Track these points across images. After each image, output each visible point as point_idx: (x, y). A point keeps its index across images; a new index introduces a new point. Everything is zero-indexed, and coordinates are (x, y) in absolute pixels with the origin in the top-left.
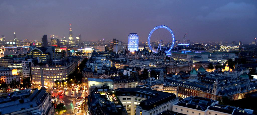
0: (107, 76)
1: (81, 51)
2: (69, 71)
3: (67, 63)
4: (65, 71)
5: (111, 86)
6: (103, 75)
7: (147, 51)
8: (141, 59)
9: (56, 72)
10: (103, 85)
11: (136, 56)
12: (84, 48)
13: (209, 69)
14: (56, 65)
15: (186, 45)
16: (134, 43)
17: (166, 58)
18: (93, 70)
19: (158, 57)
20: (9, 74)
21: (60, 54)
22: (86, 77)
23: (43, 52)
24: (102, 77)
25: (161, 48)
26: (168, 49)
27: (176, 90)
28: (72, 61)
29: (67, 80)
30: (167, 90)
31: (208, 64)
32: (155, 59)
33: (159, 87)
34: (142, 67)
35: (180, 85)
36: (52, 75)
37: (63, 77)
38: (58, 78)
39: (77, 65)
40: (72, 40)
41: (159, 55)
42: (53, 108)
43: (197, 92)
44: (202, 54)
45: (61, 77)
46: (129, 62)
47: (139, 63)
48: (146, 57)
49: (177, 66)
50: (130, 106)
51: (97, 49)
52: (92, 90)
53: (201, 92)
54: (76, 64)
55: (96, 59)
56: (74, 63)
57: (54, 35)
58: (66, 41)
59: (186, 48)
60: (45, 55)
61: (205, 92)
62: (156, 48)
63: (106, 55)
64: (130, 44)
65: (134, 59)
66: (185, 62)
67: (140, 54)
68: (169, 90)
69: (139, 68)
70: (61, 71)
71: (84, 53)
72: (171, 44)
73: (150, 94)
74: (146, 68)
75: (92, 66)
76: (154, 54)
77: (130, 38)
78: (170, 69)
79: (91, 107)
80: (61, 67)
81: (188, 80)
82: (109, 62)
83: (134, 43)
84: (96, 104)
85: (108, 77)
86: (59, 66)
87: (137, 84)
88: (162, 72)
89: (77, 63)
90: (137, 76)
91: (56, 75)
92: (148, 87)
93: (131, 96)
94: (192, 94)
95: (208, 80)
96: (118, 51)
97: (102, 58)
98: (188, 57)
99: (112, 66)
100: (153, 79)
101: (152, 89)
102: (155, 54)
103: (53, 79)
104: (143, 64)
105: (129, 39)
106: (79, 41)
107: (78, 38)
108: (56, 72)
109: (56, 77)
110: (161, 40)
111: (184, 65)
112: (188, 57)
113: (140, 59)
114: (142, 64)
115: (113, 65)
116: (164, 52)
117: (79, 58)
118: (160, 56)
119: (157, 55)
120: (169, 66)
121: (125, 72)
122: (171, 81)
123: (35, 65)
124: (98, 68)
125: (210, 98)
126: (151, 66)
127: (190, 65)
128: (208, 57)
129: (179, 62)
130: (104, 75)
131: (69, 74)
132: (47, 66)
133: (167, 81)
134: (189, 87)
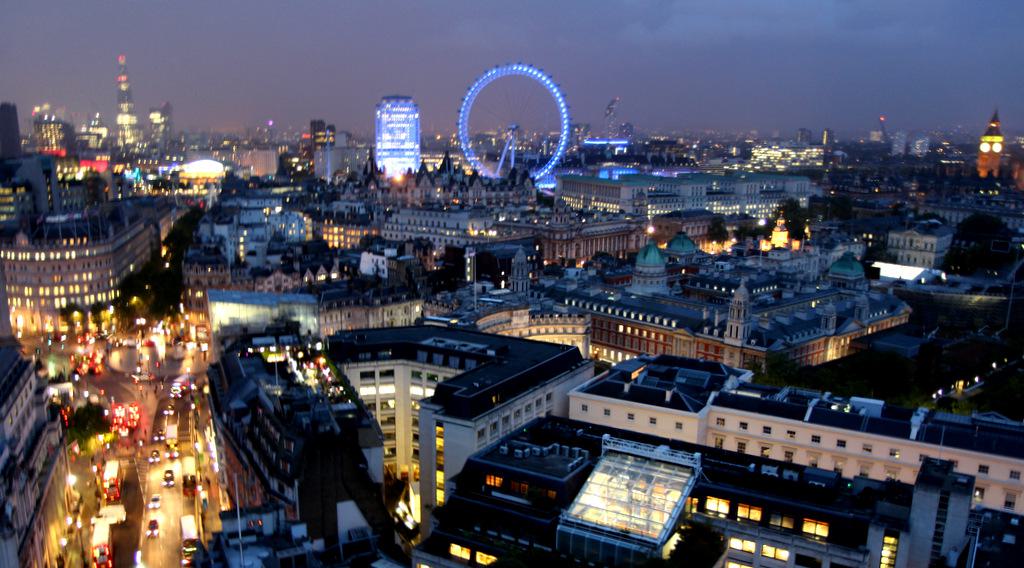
0: (289, 282)
1: (175, 174)
2: (124, 262)
3: (111, 229)
4: (104, 264)
5: (308, 321)
6: (272, 278)
7: (456, 171)
8: (433, 204)
9: (64, 269)
10: (276, 320)
11: (409, 191)
12: (187, 160)
13: (710, 240)
14: (64, 237)
15: (618, 145)
16: (403, 136)
17: (535, 199)
18: (231, 258)
19: (502, 194)
21: (81, 189)
22: (198, 285)
24: (267, 285)
26: (544, 161)
27: (581, 330)
28: (134, 220)
29: (115, 302)
30: (543, 330)
31: (707, 221)
32: (489, 203)
33: (510, 321)
34: (437, 237)
35: (595, 309)
36: (45, 280)
37: (95, 287)
38: (75, 295)
39: (158, 236)
40: (132, 127)
42: (58, 424)
43: (665, 336)
44: (682, 178)
45: (86, 289)
46: (382, 217)
47: (424, 223)
48: (451, 195)
49: (583, 231)
50: (391, 403)
51: (245, 163)
52: (229, 343)
53: (683, 335)
54: (154, 232)
55: (241, 208)
56: (142, 226)
57: (46, 107)
58: (104, 132)
59: (615, 159)
60: (10, 195)
61: (698, 334)
62: (492, 157)
63: (283, 190)
64: (384, 143)
65: (404, 206)
66: (615, 215)
67: (429, 183)
68: (551, 330)
69: (424, 243)
70: (89, 265)
71: (185, 182)
72: (556, 140)
73: (474, 349)
74: (455, 244)
75: (222, 239)
76: (486, 182)
77: (385, 117)
78: (554, 245)
79: (225, 416)
80: (87, 247)
81: (628, 290)
82: (297, 221)
83: (403, 136)
84: (247, 403)
85: (296, 283)
86: (79, 241)
87: (418, 309)
88: (520, 257)
89: (157, 227)
90: (419, 276)
91: (65, 281)
92: (467, 324)
93: (394, 362)
94: (648, 345)
95: (708, 286)
96: (335, 174)
97: (267, 202)
98: (626, 193)
99: (310, 236)
100: (484, 288)
101: (484, 329)
102: (489, 185)
103: (52, 297)
104: (442, 225)
105: (380, 121)
106: (164, 130)
107: (156, 117)
108: (64, 269)
109: (67, 289)
110: (514, 126)
111: (611, 227)
112: (626, 193)
113: (429, 206)
114: (439, 226)
115: (314, 232)
116: (526, 175)
117: (167, 205)
118: (510, 190)
119: (498, 188)
120: (550, 231)
121: (367, 263)
122: (557, 295)
124: (252, 246)
125: (716, 357)
126: (476, 233)
127: (633, 226)
129: (590, 214)
130: (278, 274)
131: (124, 274)
132: (22, 240)
133: (542, 295)
134: (633, 316)
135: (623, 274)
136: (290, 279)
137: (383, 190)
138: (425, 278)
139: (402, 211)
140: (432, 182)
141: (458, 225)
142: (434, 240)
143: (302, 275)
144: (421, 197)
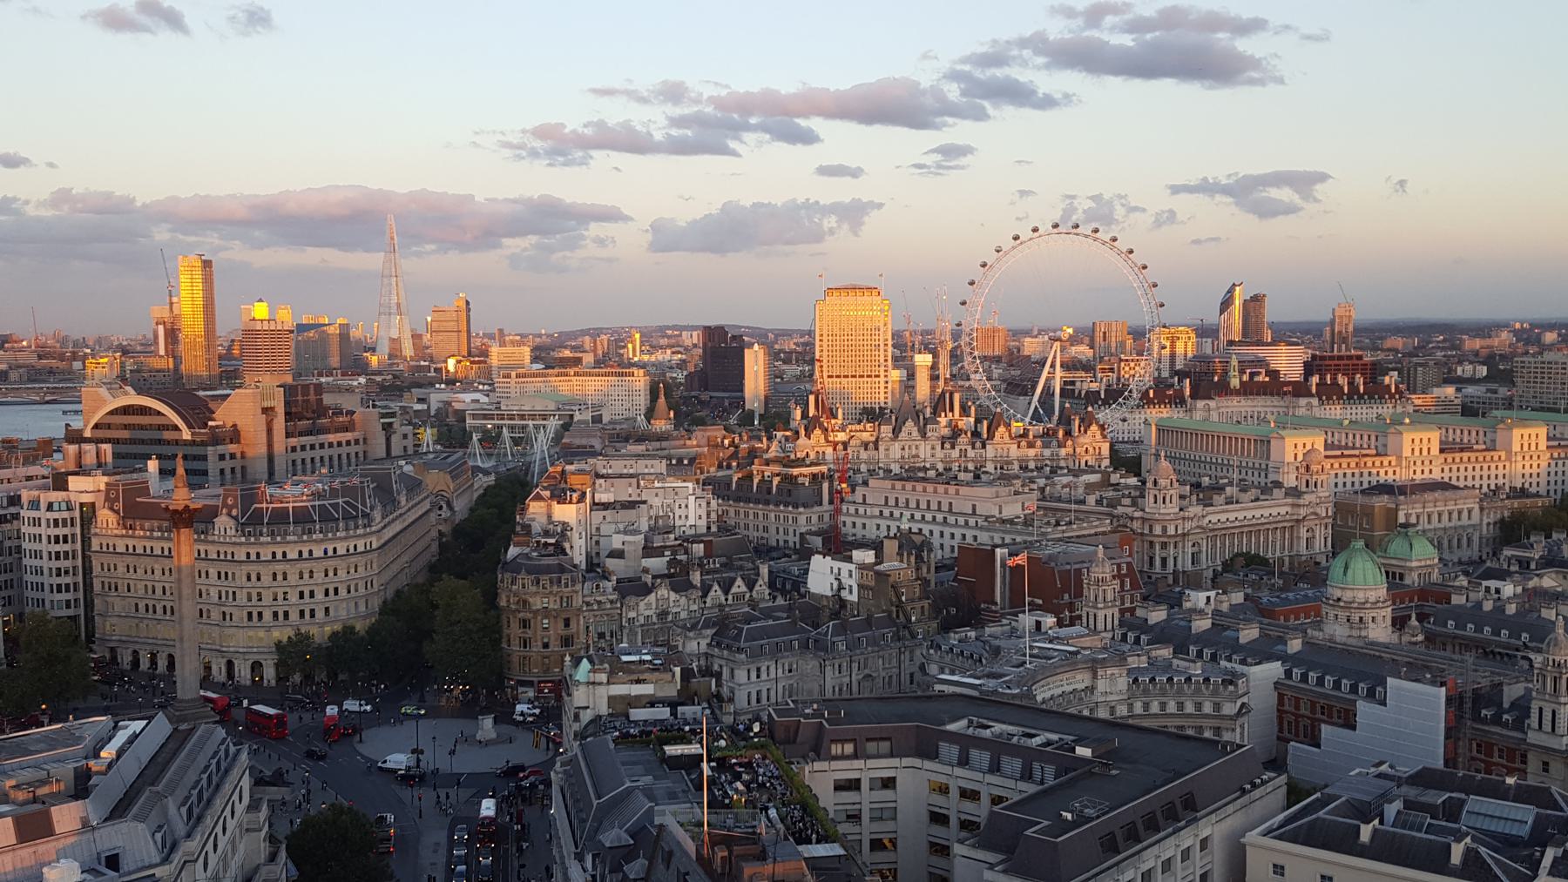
6: (652, 597)
8: (925, 469)
11: (882, 448)
17: (1106, 462)
19: (1047, 452)
23: (190, 426)
32: (1024, 468)
34: (936, 529)
41: (1055, 443)
48: (955, 454)
49: (1206, 520)
67: (915, 433)
69: (918, 539)
74: (969, 540)
93: (895, 762)
119: (1039, 443)
120: (1144, 520)
121: (822, 575)
123: (126, 528)
124: (617, 542)
128: (1435, 450)
130: (663, 592)
135: (1297, 601)
136: (683, 600)
138: (926, 603)
139: (872, 482)
140: (924, 435)
141: (974, 507)
142: (931, 532)
143: (706, 590)
144: (903, 457)
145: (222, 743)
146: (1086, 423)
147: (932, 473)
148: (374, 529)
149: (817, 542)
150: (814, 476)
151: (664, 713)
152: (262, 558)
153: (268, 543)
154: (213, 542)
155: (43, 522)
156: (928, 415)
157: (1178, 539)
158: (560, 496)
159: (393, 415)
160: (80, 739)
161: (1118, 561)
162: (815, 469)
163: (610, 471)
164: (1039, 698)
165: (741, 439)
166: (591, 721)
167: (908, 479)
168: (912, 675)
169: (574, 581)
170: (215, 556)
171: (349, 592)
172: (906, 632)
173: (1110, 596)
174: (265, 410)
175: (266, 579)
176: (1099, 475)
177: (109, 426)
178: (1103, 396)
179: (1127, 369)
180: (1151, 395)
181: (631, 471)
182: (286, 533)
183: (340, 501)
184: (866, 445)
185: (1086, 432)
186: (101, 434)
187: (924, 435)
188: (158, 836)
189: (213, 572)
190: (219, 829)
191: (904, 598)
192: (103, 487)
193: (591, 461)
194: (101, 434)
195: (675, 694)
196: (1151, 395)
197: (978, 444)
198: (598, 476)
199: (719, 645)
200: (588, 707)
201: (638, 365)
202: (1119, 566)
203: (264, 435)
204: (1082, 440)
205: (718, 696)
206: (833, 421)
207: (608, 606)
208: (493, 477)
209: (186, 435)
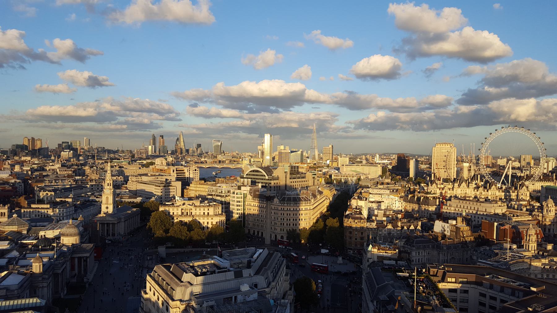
8: (469, 197)
17: (528, 198)
20: (208, 213)
23: (268, 176)
25: (512, 175)
137: (440, 188)
145: (280, 257)
146: (522, 186)
147: (471, 199)
148: (312, 204)
149: (435, 216)
150: (434, 198)
151: (393, 262)
152: (285, 210)
153: (286, 206)
154: (273, 205)
155: (235, 197)
156: (469, 181)
157: (554, 223)
158: (360, 198)
159: (315, 175)
160: (248, 253)
161: (536, 229)
162: (434, 195)
163: (373, 192)
164: (512, 270)
165: (411, 185)
166: (372, 262)
167: (465, 200)
168: (467, 259)
169: (364, 222)
170: (274, 208)
171: (305, 220)
172: (465, 246)
173: (534, 240)
174: (285, 172)
175: (285, 215)
176: (526, 202)
177: (250, 175)
178: (525, 178)
179: (533, 170)
180: (542, 178)
181: (379, 193)
182: (290, 204)
183: (304, 196)
184: (449, 189)
185: (522, 188)
186: (248, 176)
187: (468, 186)
188: (266, 280)
189: (273, 212)
190: (279, 280)
191: (465, 235)
192: (249, 190)
193: (368, 189)
194: (248, 176)
195: (397, 257)
196: (542, 178)
197: (486, 191)
198: (370, 193)
199: (407, 244)
200: (371, 258)
201: (380, 164)
202: (536, 231)
203: (285, 178)
204: (520, 191)
205: (409, 259)
206: (439, 182)
207: (374, 230)
208: (340, 192)
209: (267, 178)
